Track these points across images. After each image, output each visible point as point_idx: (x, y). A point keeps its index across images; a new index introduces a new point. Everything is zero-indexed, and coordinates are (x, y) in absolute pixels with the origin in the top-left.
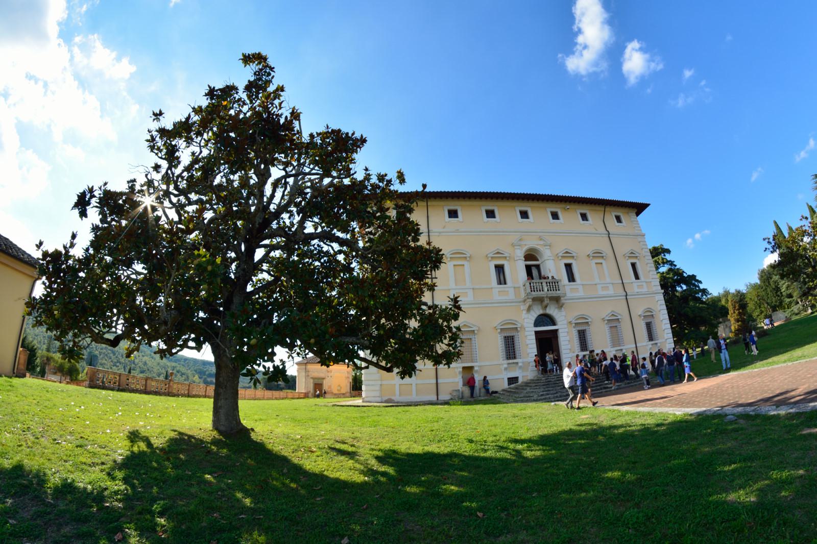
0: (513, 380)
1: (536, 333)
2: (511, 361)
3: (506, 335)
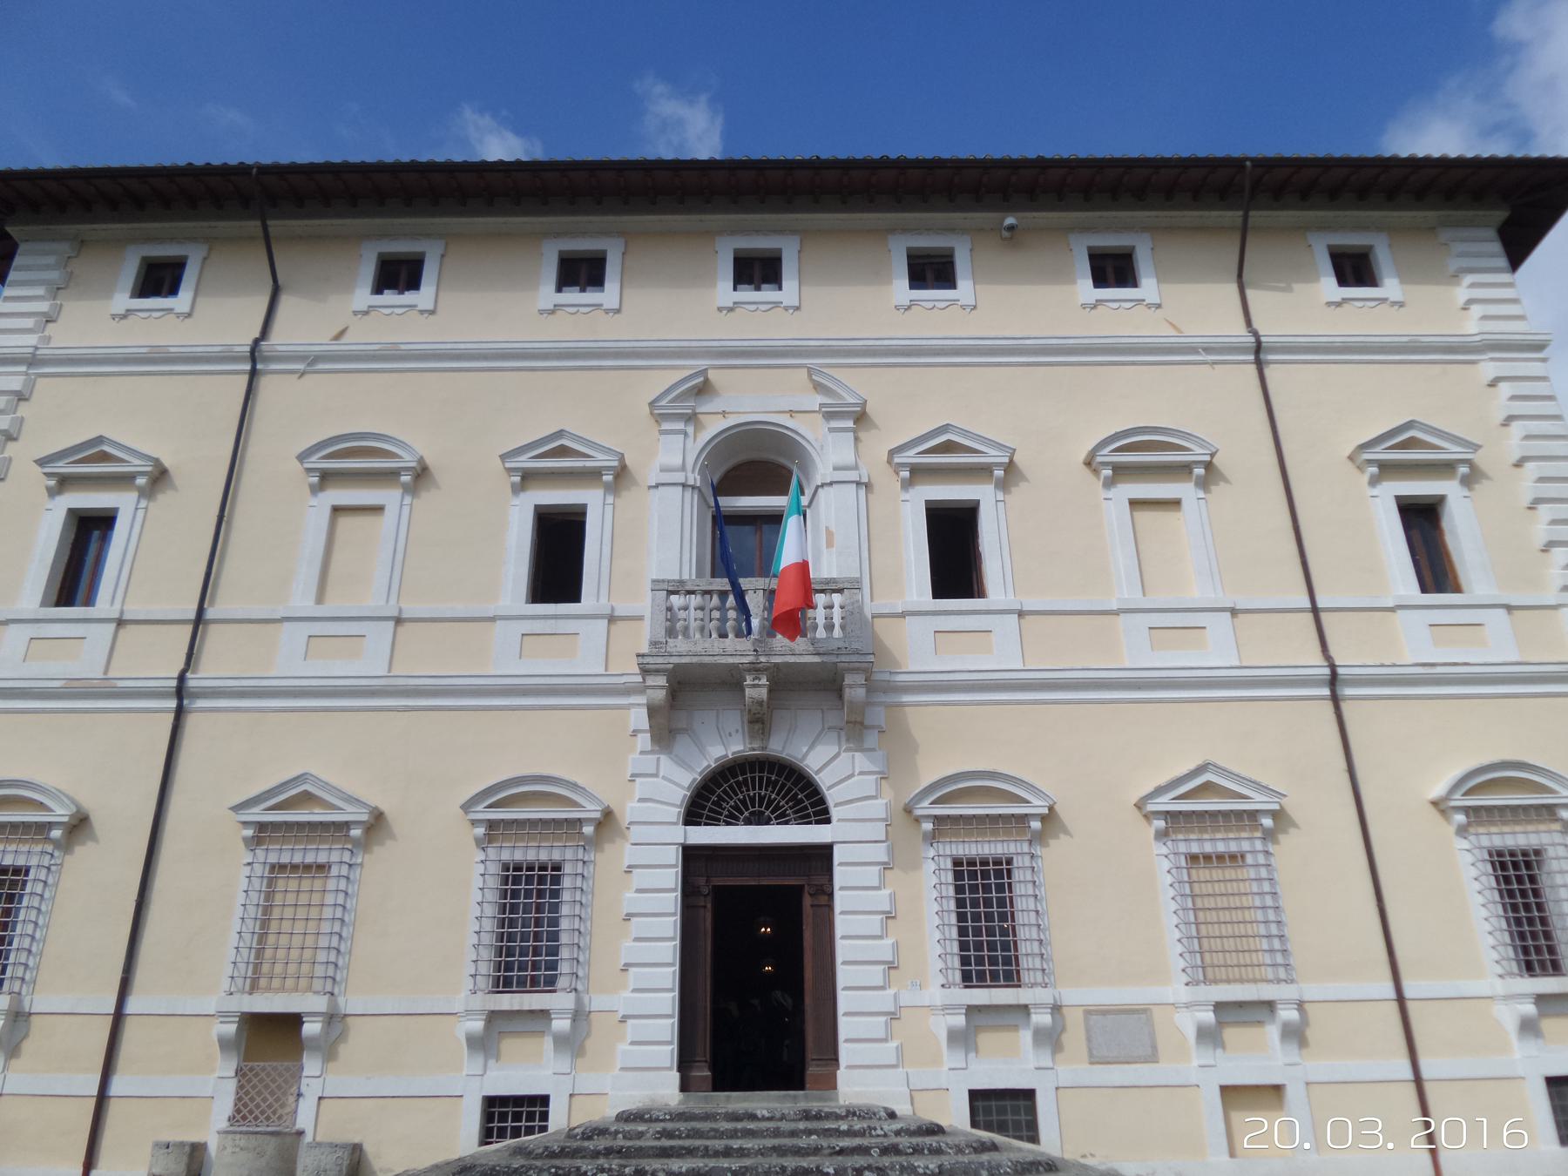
0: (510, 1114)
1: (691, 855)
2: (508, 1002)
3: (506, 856)
